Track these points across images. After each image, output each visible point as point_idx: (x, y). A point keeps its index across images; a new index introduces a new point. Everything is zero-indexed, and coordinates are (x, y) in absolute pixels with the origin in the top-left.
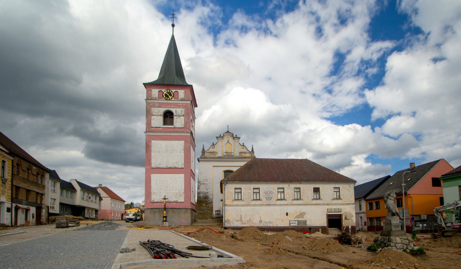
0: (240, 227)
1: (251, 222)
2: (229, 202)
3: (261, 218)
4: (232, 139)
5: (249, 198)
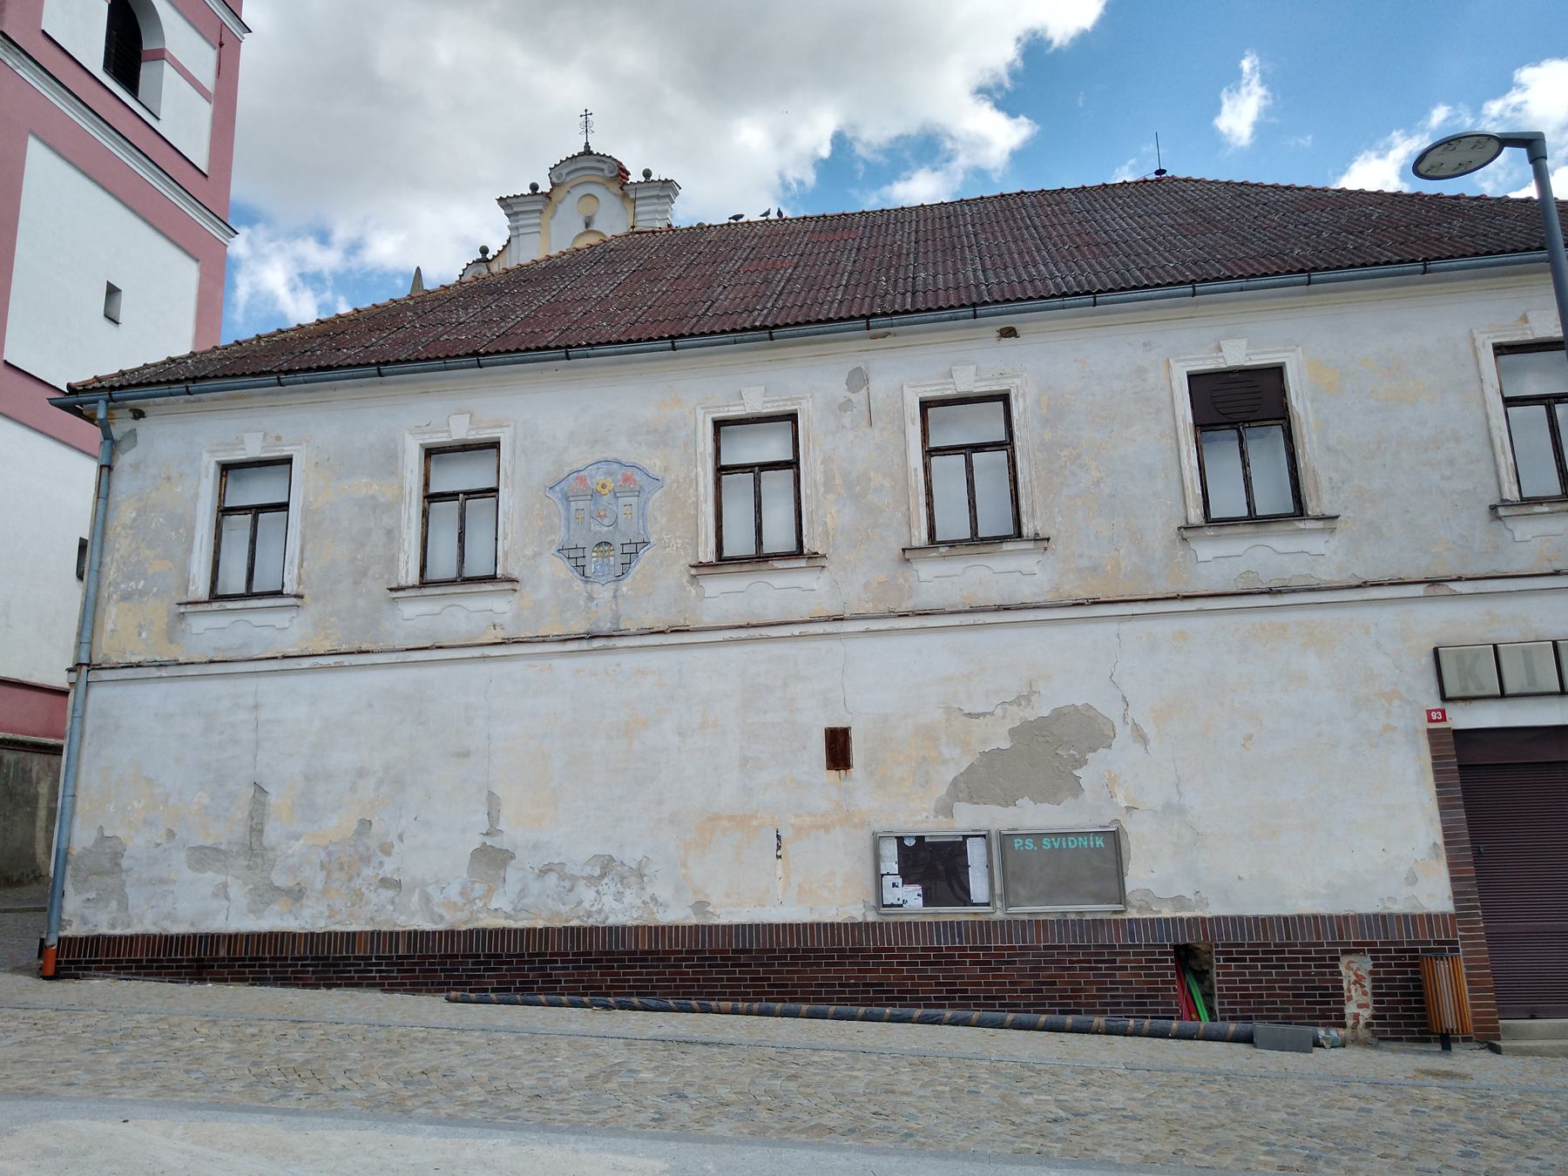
0: (233, 938)
1: (368, 872)
2: (140, 626)
3: (493, 814)
4: (617, 201)
5: (364, 574)
